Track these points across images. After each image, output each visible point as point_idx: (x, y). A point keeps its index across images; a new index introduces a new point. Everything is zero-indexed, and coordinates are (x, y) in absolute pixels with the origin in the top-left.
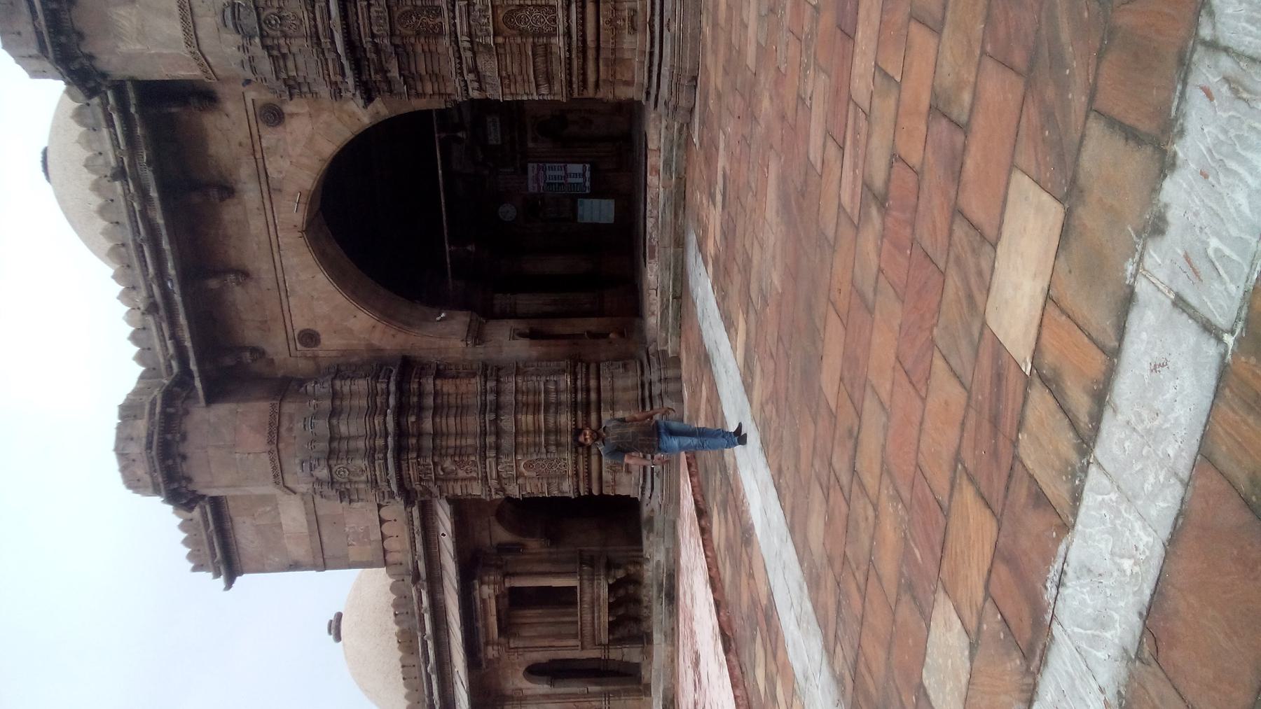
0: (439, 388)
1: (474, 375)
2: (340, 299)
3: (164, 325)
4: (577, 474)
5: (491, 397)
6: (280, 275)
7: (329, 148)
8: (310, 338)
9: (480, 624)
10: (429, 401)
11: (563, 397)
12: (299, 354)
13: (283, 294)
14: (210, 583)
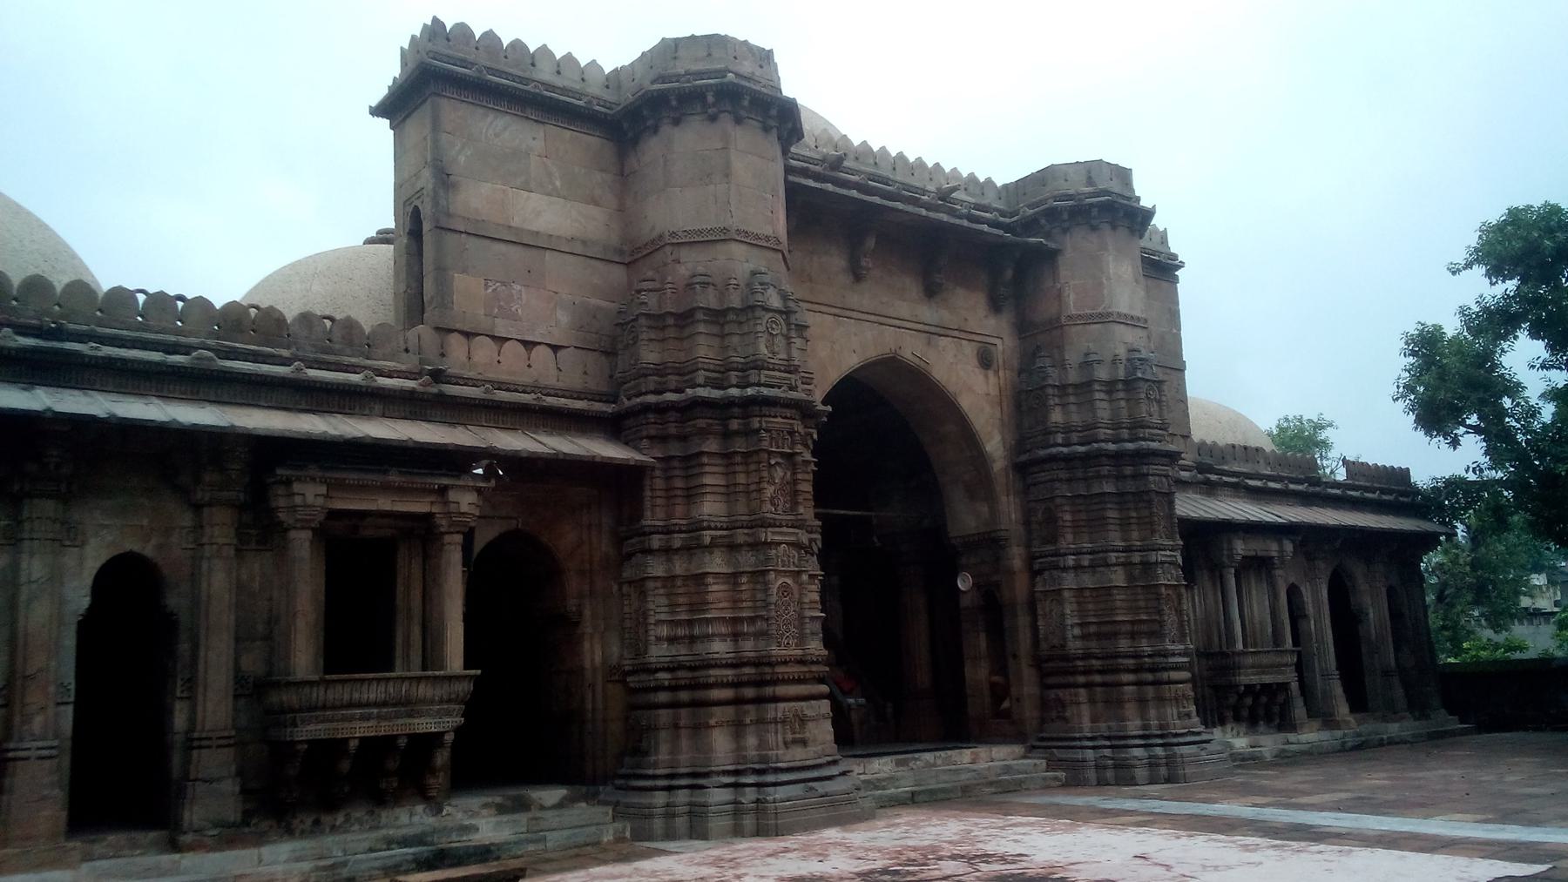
6: (854, 314)
7: (966, 403)
9: (394, 478)
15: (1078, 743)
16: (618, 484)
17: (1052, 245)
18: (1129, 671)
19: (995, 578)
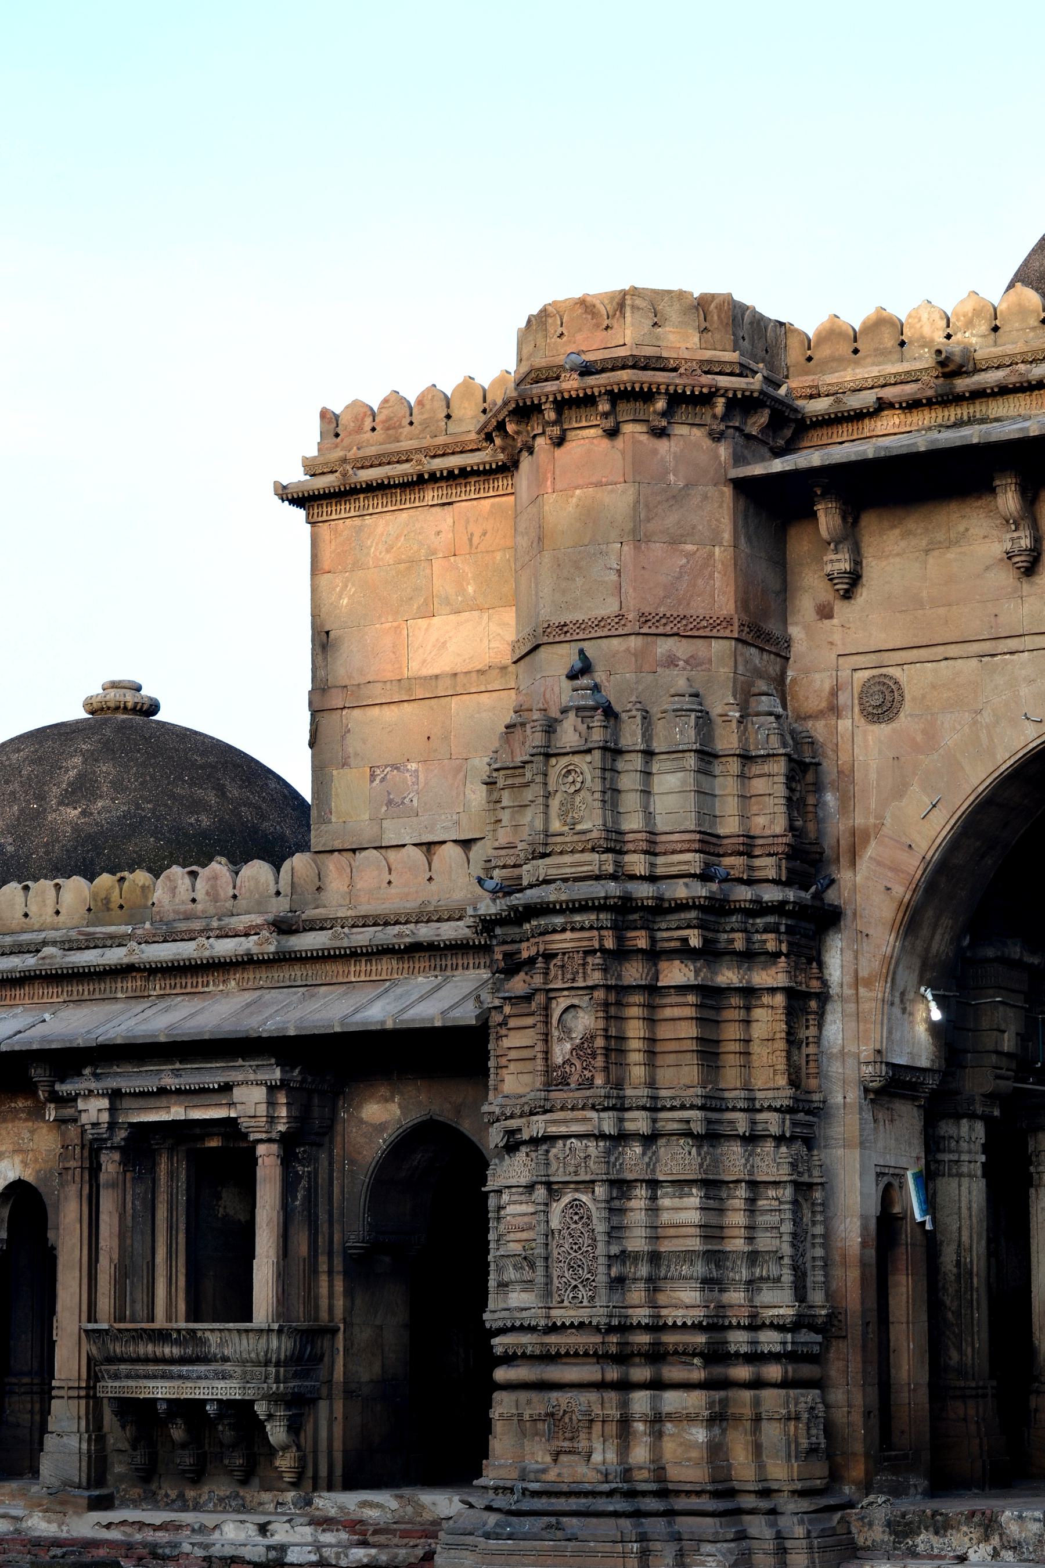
0: (766, 999)
1: (794, 1082)
2: (977, 776)
3: (910, 389)
4: (553, 1329)
5: (741, 1123)
6: (1029, 642)
8: (883, 703)
10: (728, 976)
11: (736, 1297)
12: (845, 674)
14: (293, 451)
16: (455, 1054)
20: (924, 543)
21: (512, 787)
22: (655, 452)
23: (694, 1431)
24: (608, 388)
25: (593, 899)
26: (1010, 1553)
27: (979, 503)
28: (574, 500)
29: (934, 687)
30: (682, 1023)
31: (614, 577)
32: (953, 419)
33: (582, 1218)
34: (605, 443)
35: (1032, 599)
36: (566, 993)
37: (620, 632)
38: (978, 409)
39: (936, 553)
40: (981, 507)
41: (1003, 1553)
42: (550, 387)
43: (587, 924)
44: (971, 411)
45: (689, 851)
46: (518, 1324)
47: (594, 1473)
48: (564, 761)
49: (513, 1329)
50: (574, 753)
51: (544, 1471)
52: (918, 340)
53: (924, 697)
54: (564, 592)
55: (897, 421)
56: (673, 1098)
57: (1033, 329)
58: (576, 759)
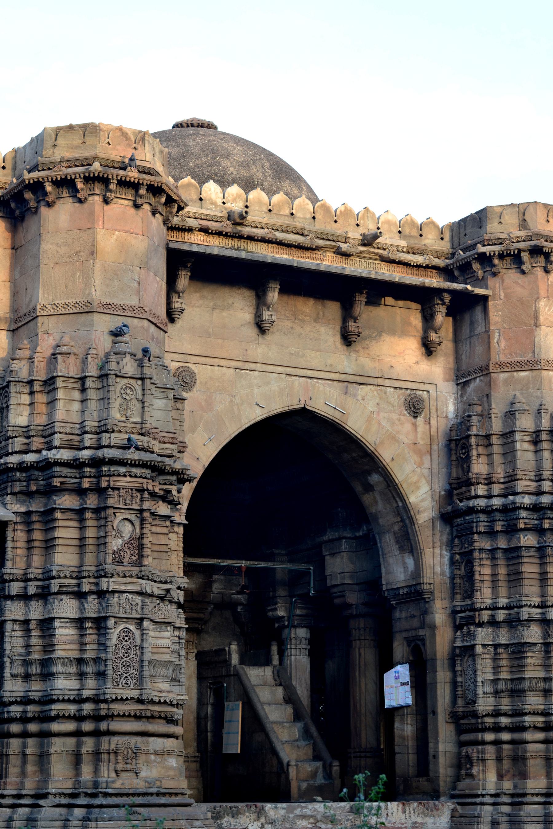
2: (232, 430)
6: (259, 367)
7: (386, 454)
13: (239, 365)
15: (478, 800)
17: (480, 291)
18: (536, 728)
19: (421, 632)
20: (211, 304)
21: (66, 388)
22: (152, 223)
23: (170, 760)
24: (152, 183)
25: (151, 462)
26: (270, 826)
27: (239, 291)
28: (115, 237)
29: (211, 379)
30: (161, 536)
31: (137, 285)
32: (230, 245)
33: (129, 639)
34: (133, 211)
35: (263, 346)
36: (123, 511)
37: (141, 316)
38: (242, 244)
39: (217, 311)
40: (240, 294)
41: (266, 826)
42: (121, 172)
43: (138, 475)
44: (239, 244)
45: (169, 443)
46: (66, 698)
47: (144, 783)
48: (125, 381)
49: (63, 701)
50: (130, 378)
51: (113, 782)
52: (209, 200)
53: (206, 383)
54: (108, 286)
55: (202, 238)
56: (160, 576)
57: (265, 212)
58: (132, 382)
